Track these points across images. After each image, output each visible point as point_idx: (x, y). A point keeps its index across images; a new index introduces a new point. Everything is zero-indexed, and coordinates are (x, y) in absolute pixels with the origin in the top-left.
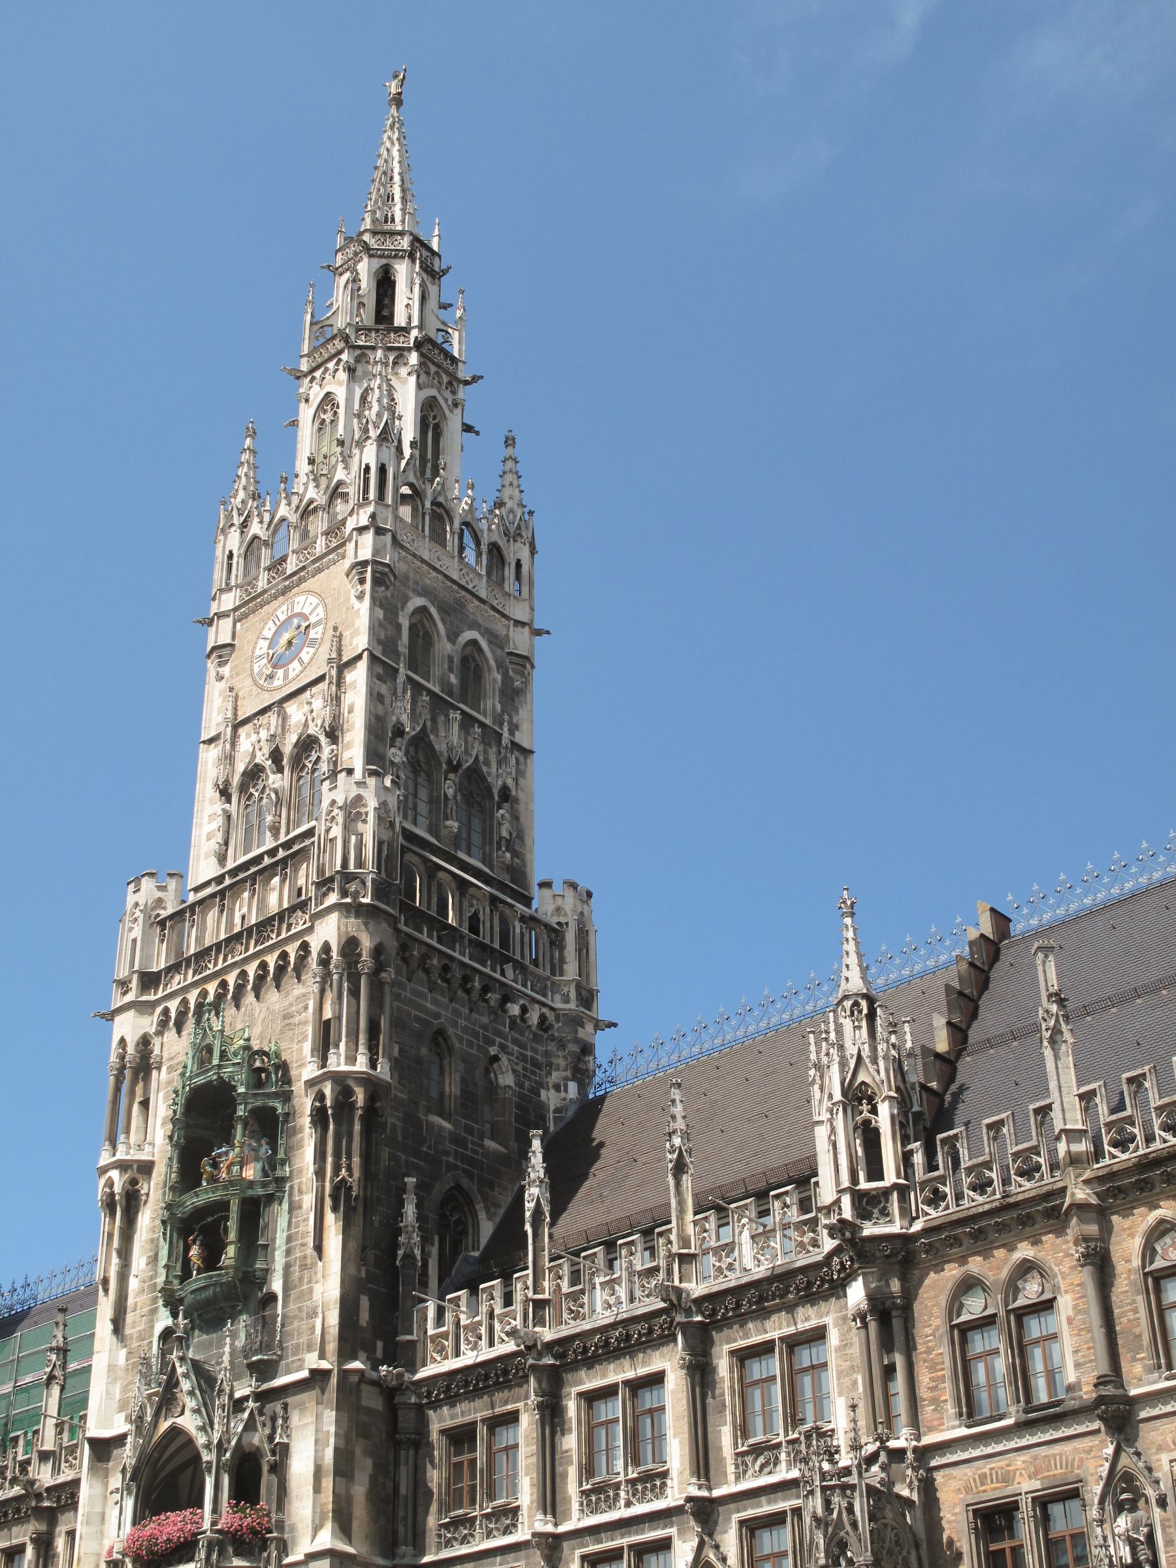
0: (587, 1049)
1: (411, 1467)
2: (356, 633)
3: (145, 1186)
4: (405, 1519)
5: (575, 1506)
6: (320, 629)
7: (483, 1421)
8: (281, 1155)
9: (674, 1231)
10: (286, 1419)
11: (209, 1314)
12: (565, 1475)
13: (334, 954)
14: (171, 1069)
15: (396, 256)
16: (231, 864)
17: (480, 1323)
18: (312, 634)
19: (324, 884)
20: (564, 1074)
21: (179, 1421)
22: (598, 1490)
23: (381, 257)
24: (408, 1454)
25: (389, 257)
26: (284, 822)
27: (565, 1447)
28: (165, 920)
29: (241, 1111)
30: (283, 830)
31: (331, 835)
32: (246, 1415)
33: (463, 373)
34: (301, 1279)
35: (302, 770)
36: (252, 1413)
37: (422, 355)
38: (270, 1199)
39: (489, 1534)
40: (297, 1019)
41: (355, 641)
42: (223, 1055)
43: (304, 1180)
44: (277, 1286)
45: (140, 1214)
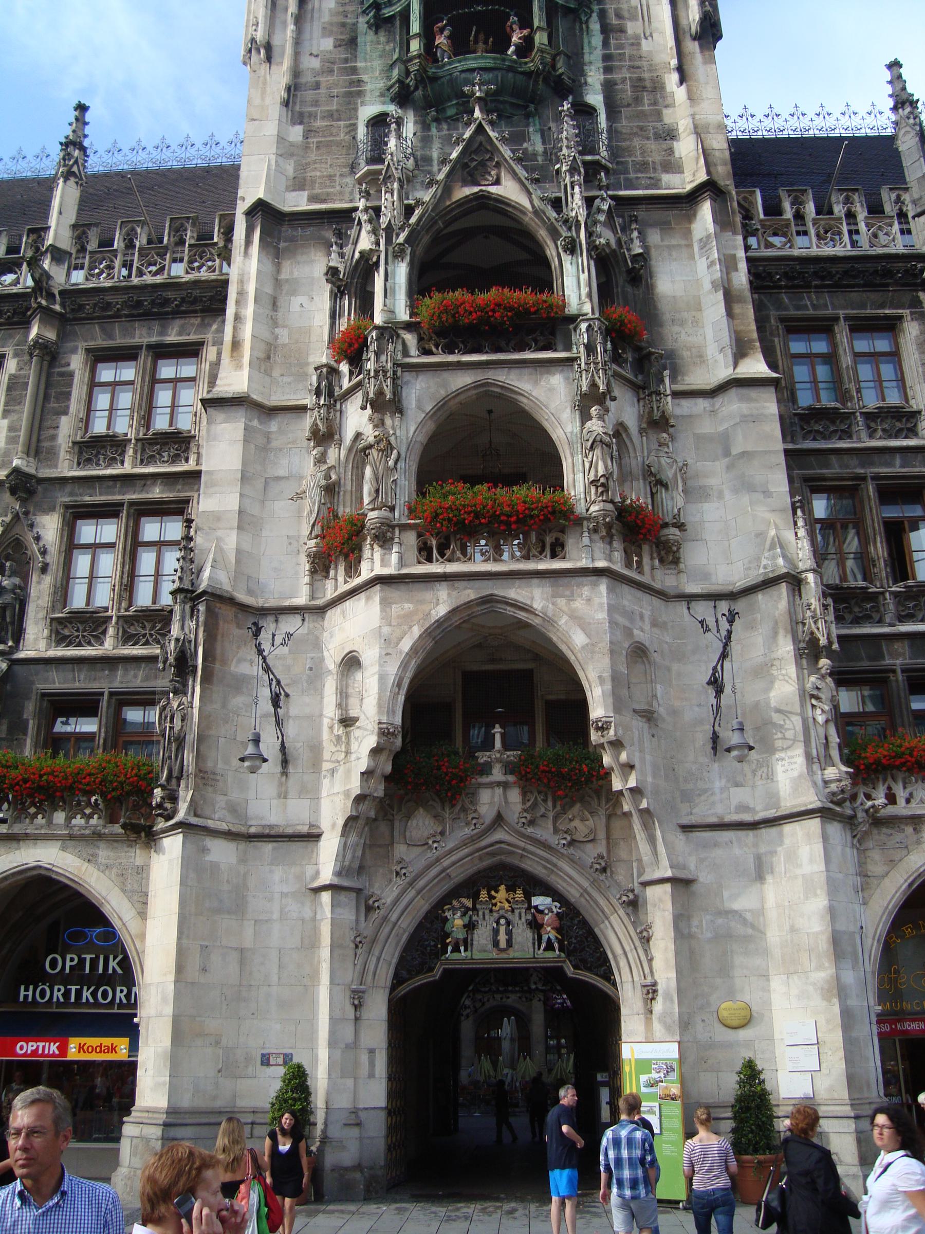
7: (846, 319)
21: (493, 189)
34: (637, 100)
39: (871, 436)
44: (595, 98)
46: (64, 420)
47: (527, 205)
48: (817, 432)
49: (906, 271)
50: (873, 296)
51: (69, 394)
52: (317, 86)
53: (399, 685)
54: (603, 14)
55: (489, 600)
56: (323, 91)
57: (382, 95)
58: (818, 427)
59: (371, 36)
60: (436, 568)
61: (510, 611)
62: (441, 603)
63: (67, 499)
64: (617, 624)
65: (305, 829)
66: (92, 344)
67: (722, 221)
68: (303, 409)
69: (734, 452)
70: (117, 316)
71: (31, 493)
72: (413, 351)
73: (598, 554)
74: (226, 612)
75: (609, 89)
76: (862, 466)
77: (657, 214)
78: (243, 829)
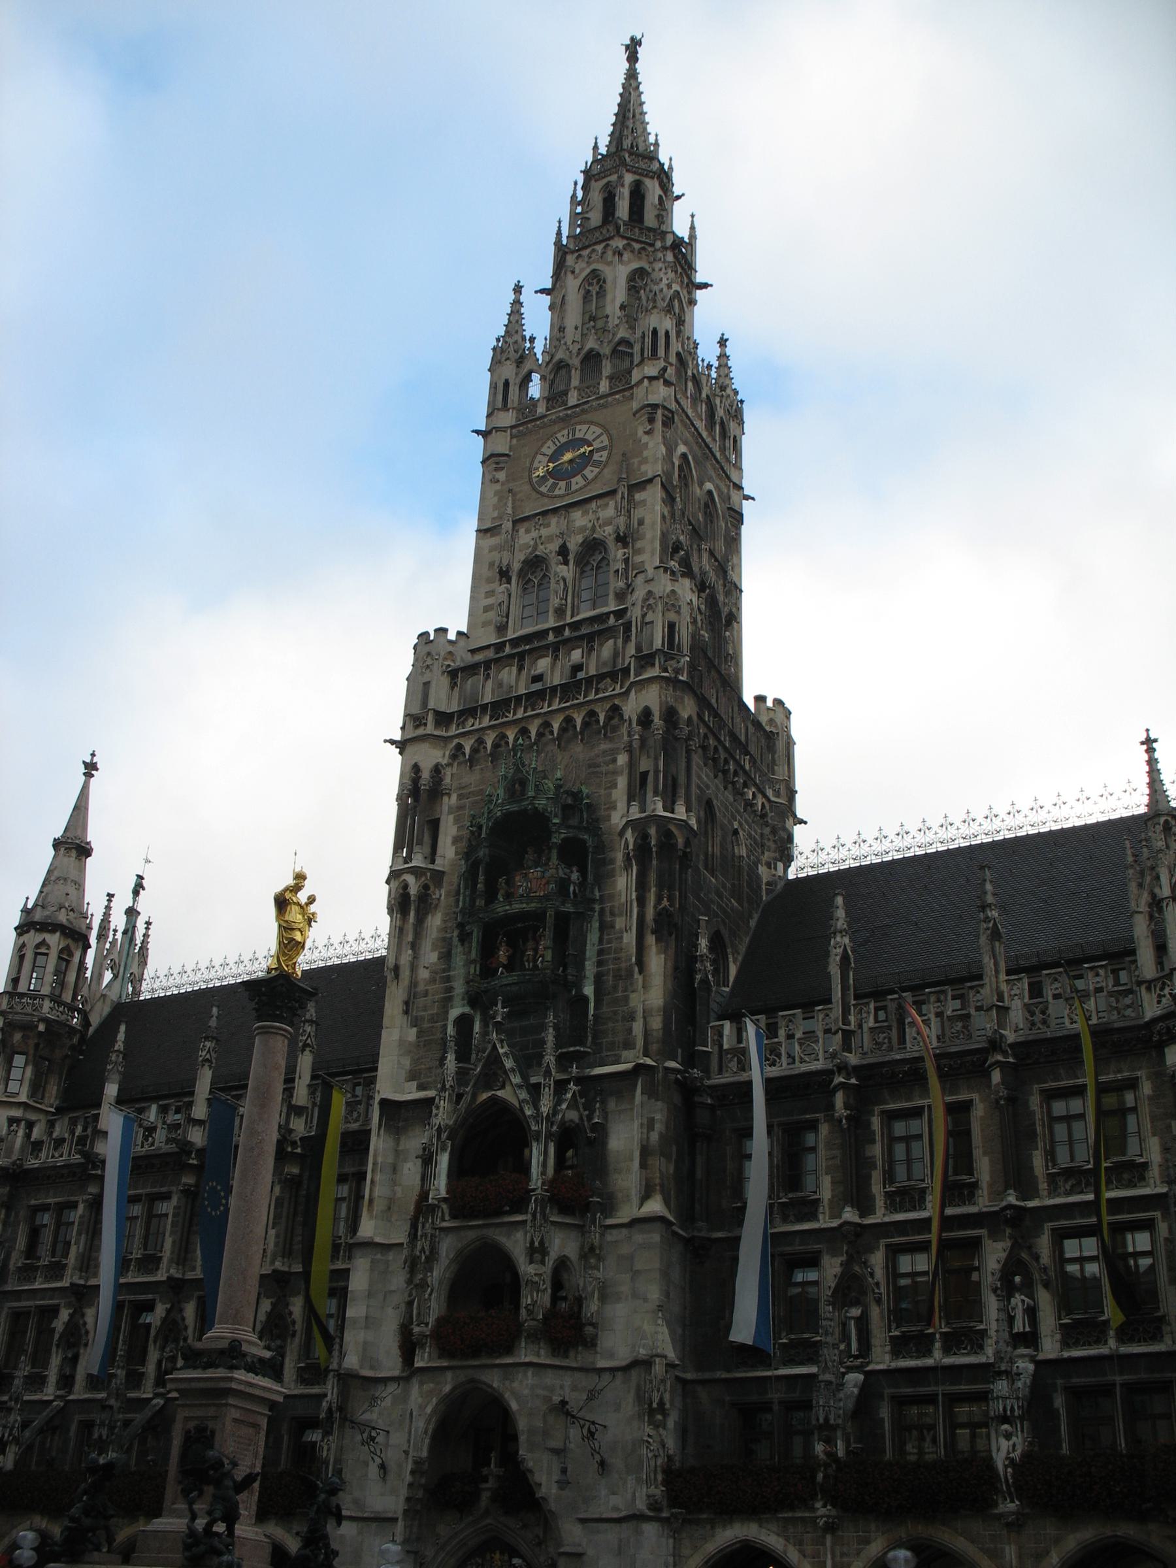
0: (790, 838)
2: (645, 461)
3: (437, 892)
5: (880, 1203)
6: (605, 453)
8: (590, 878)
9: (988, 986)
10: (603, 1102)
11: (526, 1005)
12: (870, 1177)
13: (656, 719)
14: (460, 797)
15: (646, 176)
16: (511, 635)
17: (779, 1043)
18: (596, 457)
19: (645, 660)
20: (773, 855)
21: (499, 1093)
22: (903, 1192)
23: (635, 173)
25: (640, 174)
26: (569, 605)
27: (868, 1154)
29: (556, 839)
30: (569, 613)
31: (647, 619)
32: (569, 1096)
33: (699, 278)
34: (615, 987)
35: (586, 565)
36: (574, 1095)
37: (675, 256)
38: (583, 917)
40: (604, 769)
41: (643, 468)
42: (537, 788)
44: (589, 990)
45: (430, 917)
52: (426, 994)
53: (426, 1432)
54: (602, 911)
55: (472, 1381)
56: (430, 998)
57: (463, 999)
59: (460, 949)
61: (484, 1387)
65: (390, 1515)
67: (651, 1092)
69: (635, 1268)
72: (447, 1218)
78: (360, 1515)
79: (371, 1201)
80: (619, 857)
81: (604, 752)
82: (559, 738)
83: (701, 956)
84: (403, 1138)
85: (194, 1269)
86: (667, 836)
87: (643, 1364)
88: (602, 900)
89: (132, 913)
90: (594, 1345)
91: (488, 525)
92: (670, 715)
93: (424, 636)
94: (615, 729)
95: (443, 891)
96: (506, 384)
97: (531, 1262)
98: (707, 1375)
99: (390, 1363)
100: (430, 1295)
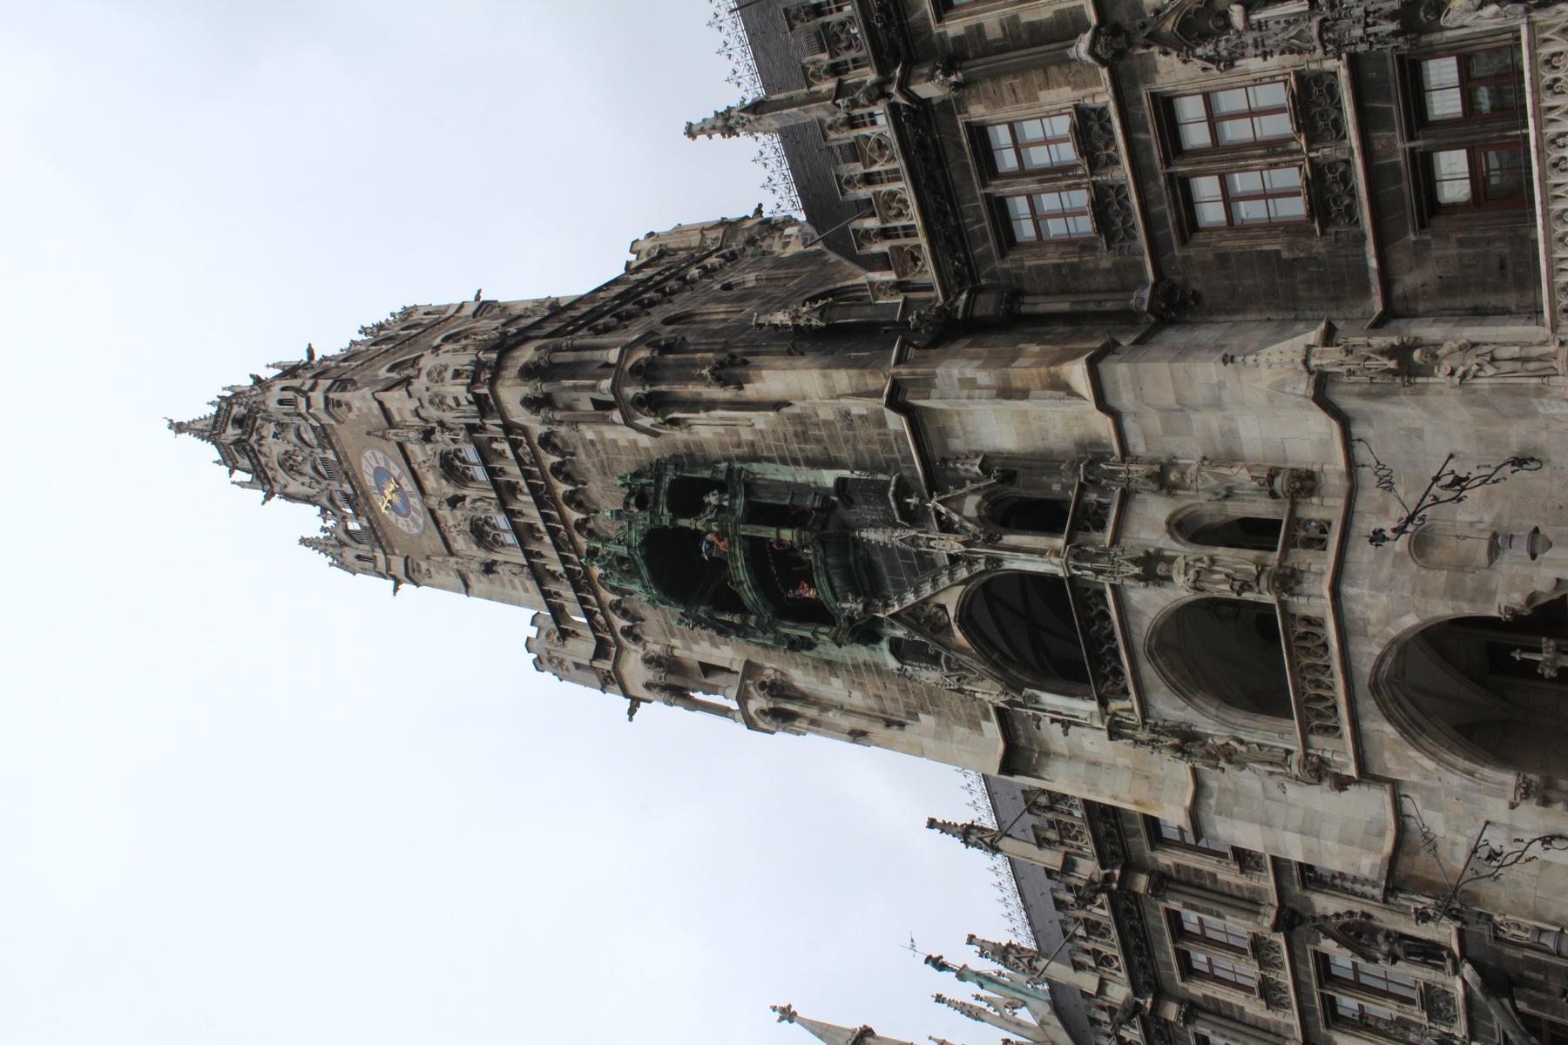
1: (1042, 299)
3: (769, 672)
4: (1099, 302)
7: (984, 185)
14: (673, 635)
21: (952, 613)
24: (1030, 305)
27: (998, 33)
28: (560, 629)
29: (666, 521)
31: (453, 404)
34: (818, 440)
38: (751, 487)
39: (1113, 161)
43: (728, 439)
44: (828, 478)
45: (796, 684)
46: (1220, 877)
47: (960, 589)
48: (1124, 222)
49: (914, 125)
50: (951, 155)
51: (1198, 872)
53: (1471, 774)
54: (741, 459)
55: (1375, 687)
56: (882, 693)
58: (1119, 221)
60: (1346, 729)
61: (1385, 668)
62: (1381, 730)
63: (1297, 889)
64: (1392, 579)
66: (1146, 846)
68: (1195, 772)
70: (1117, 826)
71: (1294, 912)
72: (1127, 704)
73: (1316, 592)
74: (1404, 864)
75: (813, 463)
76: (1156, 178)
77: (934, 439)
79: (1136, 803)
80: (679, 435)
81: (589, 456)
82: (587, 511)
83: (793, 319)
84: (1053, 748)
85: (1289, 1027)
86: (644, 372)
87: (1322, 392)
88: (728, 459)
89: (962, 974)
90: (1310, 476)
91: (459, 582)
92: (528, 373)
93: (539, 664)
94: (565, 444)
95: (768, 665)
96: (359, 557)
97: (1169, 579)
98: (1374, 277)
99: (1371, 804)
100: (1241, 742)
